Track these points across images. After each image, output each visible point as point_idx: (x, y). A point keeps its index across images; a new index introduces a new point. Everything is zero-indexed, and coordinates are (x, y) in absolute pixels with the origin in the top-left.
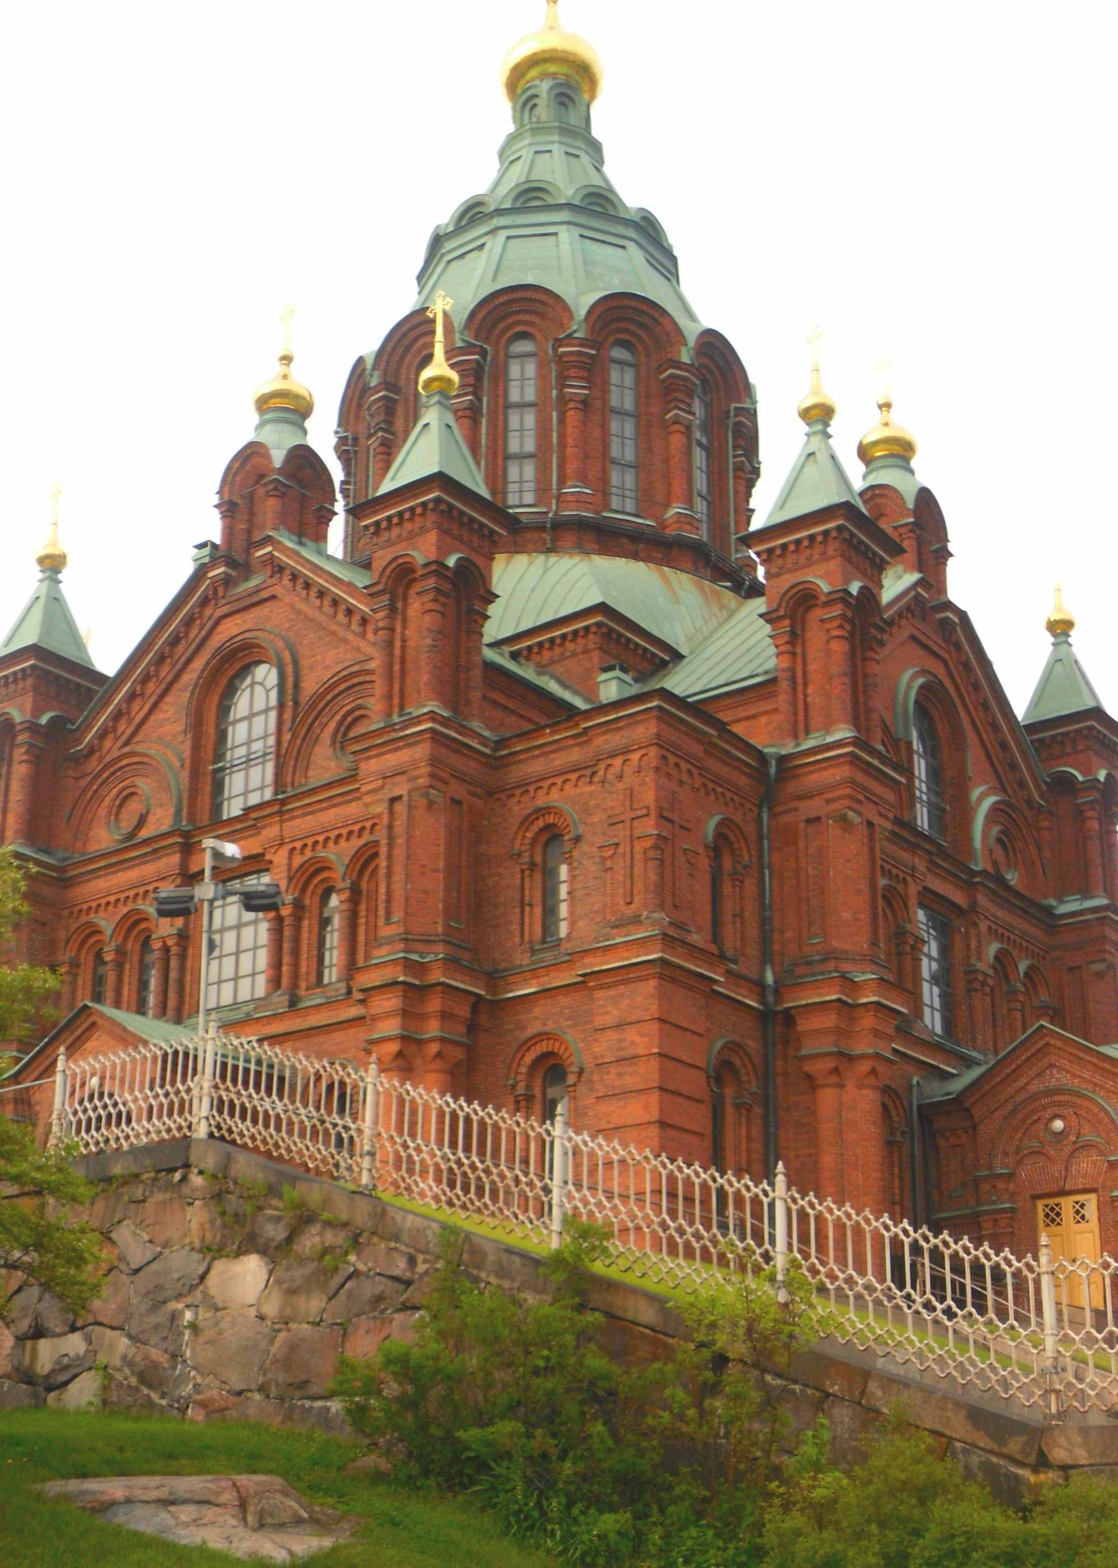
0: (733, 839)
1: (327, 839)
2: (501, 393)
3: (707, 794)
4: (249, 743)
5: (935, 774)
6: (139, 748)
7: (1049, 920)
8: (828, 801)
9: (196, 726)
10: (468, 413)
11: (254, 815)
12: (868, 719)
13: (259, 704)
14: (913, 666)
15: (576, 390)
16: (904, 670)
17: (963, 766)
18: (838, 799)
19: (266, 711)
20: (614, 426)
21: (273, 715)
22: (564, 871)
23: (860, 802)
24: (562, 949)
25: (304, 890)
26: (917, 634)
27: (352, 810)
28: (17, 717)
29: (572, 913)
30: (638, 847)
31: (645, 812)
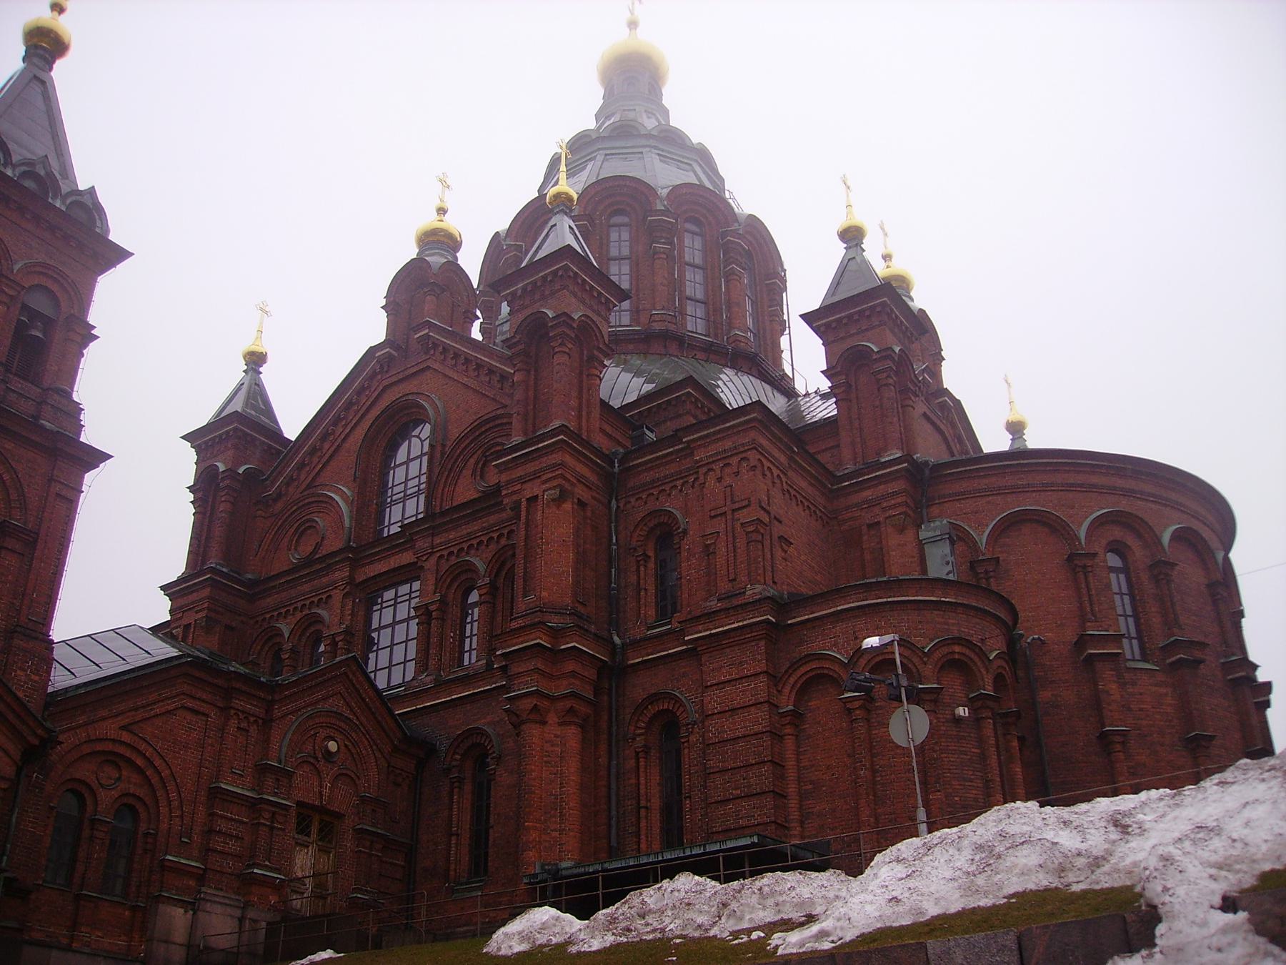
13: (416, 452)
18: (894, 507)
19: (420, 457)
20: (688, 276)
21: (425, 459)
25: (449, 587)
28: (222, 467)
31: (745, 503)
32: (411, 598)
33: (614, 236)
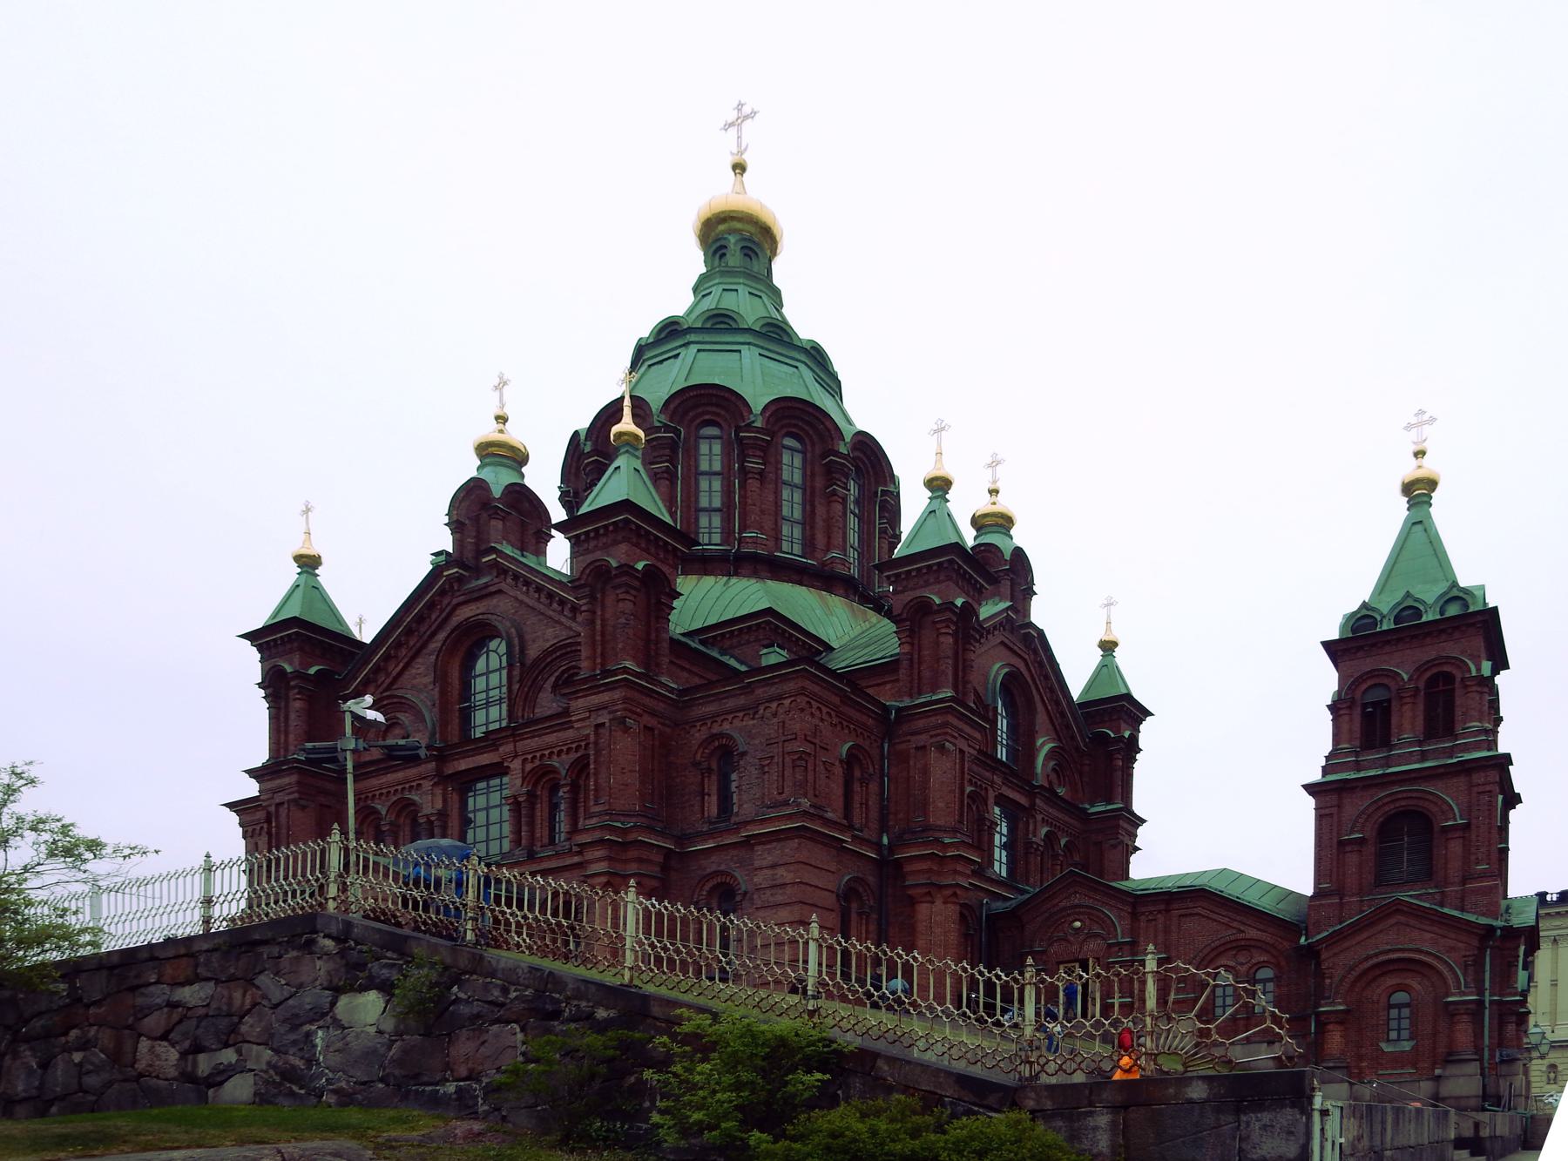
0: (861, 757)
1: (552, 753)
2: (692, 463)
3: (843, 729)
4: (487, 690)
5: (1013, 729)
6: (400, 693)
7: (1084, 816)
8: (931, 737)
9: (441, 678)
10: (666, 475)
11: (492, 737)
12: (964, 687)
14: (1001, 660)
15: (754, 464)
16: (994, 664)
17: (1032, 724)
21: (504, 672)
22: (734, 776)
23: (956, 738)
24: (732, 821)
26: (1006, 641)
27: (570, 734)
29: (740, 800)
30: (787, 759)
32: (501, 790)
33: (704, 448)
